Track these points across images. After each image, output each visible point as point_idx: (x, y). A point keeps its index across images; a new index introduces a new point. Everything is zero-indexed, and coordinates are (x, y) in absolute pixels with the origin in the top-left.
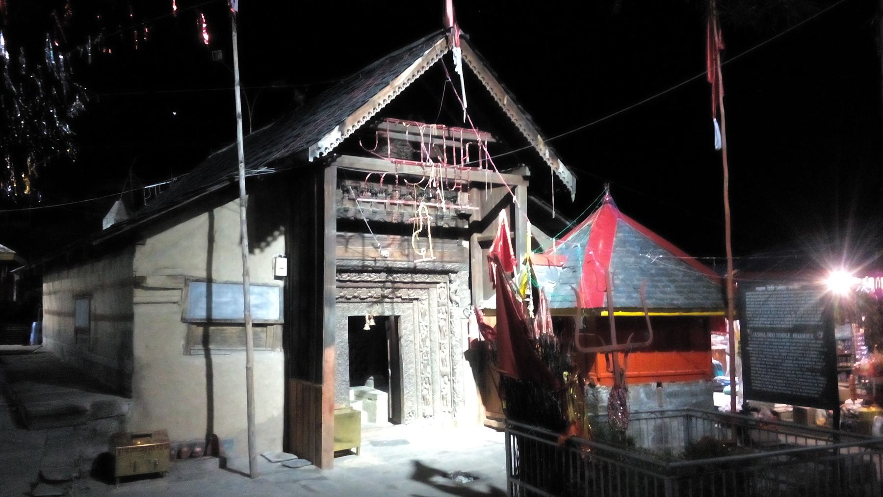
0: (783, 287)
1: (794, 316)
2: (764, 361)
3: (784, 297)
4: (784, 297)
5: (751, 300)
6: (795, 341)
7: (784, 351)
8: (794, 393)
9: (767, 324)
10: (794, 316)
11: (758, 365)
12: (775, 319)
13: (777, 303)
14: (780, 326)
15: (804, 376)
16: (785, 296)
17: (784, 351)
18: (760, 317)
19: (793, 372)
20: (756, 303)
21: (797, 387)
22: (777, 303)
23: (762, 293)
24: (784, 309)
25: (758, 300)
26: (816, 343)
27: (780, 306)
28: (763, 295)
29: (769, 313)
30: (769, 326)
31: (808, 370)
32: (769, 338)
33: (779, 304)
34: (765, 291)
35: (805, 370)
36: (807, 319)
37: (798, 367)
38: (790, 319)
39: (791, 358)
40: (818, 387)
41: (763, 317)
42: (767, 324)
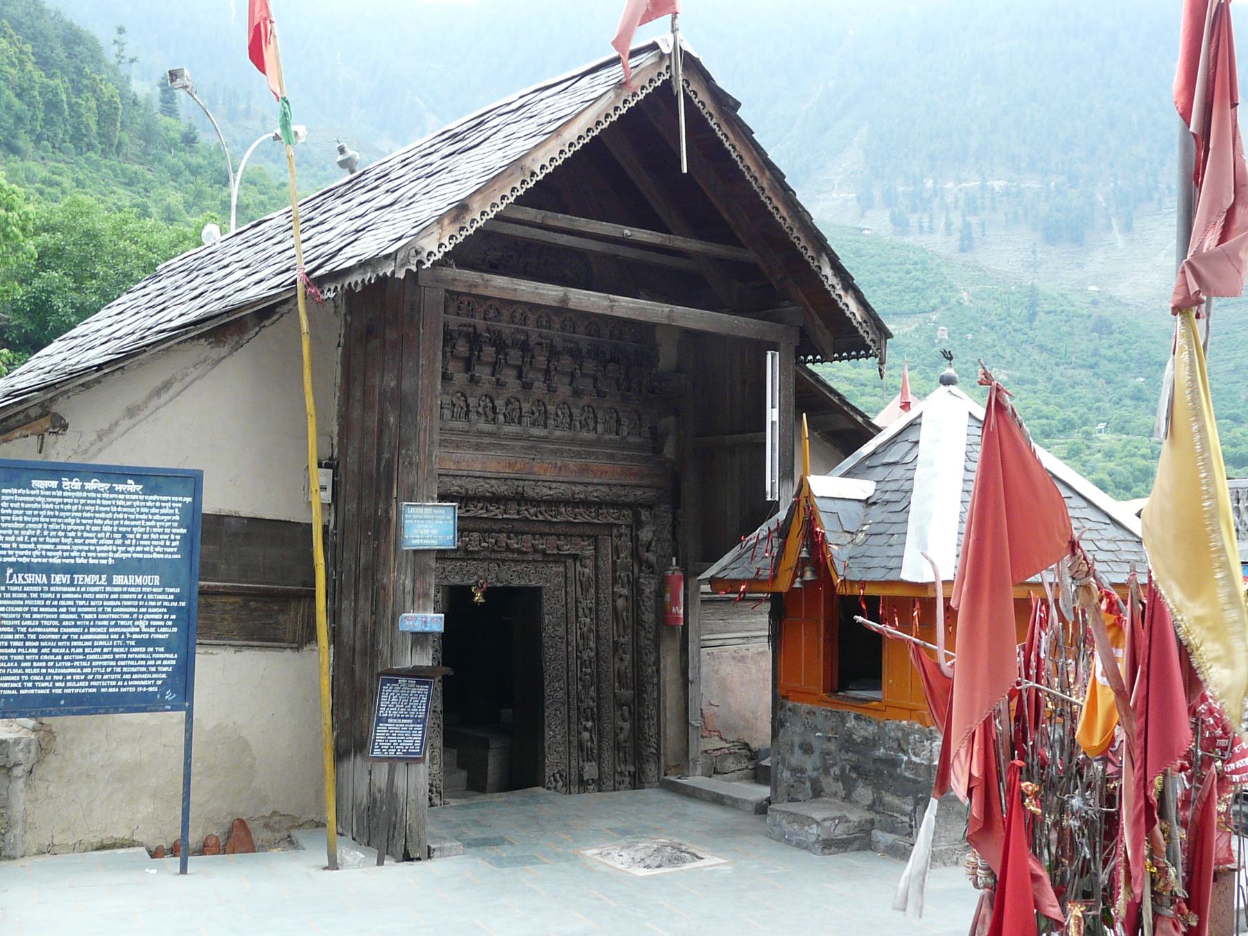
0: (103, 485)
1: (119, 542)
2: (33, 633)
3: (101, 505)
4: (101, 505)
5: (17, 505)
6: (116, 589)
7: (90, 610)
8: (103, 690)
9: (53, 557)
10: (119, 542)
11: (16, 644)
12: (75, 548)
13: (85, 514)
14: (85, 561)
15: (130, 656)
16: (104, 502)
17: (90, 610)
18: (36, 543)
19: (105, 650)
20: (29, 512)
21: (113, 677)
22: (85, 514)
23: (48, 493)
24: (98, 528)
25: (36, 506)
26: (163, 593)
27: (90, 522)
28: (51, 496)
29: (60, 534)
30: (59, 561)
31: (140, 643)
32: (55, 585)
33: (91, 518)
34: (55, 490)
35: (133, 643)
36: (147, 549)
37: (119, 639)
38: (110, 548)
39: (106, 623)
40: (157, 672)
41: (44, 543)
42: (53, 557)
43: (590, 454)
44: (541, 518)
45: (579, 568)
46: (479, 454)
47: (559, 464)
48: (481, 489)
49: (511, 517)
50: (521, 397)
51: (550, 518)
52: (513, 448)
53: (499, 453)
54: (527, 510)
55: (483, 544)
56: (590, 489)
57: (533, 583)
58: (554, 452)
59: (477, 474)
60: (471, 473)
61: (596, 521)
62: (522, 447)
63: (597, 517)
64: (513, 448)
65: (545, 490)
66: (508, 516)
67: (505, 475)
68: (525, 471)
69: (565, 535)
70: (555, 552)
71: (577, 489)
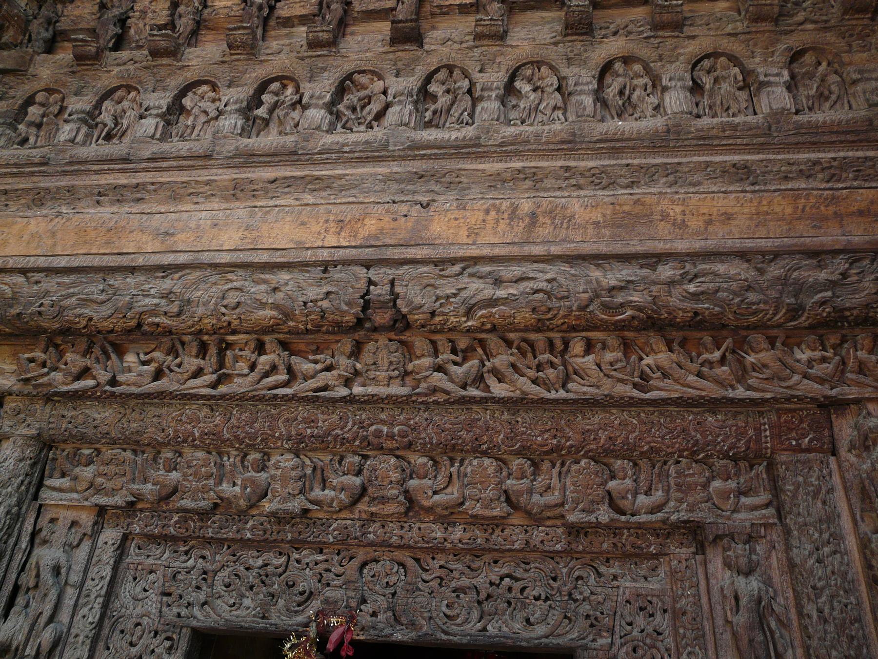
43: (650, 174)
44: (499, 390)
45: (722, 577)
46: (240, 210)
47: (526, 206)
48: (232, 298)
49: (383, 391)
50: (386, 67)
51: (534, 389)
52: (355, 184)
53: (309, 198)
54: (439, 369)
55: (317, 493)
56: (666, 271)
57: (540, 630)
58: (497, 181)
59: (225, 258)
60: (206, 258)
61: (740, 392)
62: (387, 179)
63: (742, 374)
64: (355, 184)
65: (475, 285)
66: (371, 390)
67: (324, 255)
68: (401, 237)
69: (629, 453)
70: (604, 515)
71: (611, 277)
